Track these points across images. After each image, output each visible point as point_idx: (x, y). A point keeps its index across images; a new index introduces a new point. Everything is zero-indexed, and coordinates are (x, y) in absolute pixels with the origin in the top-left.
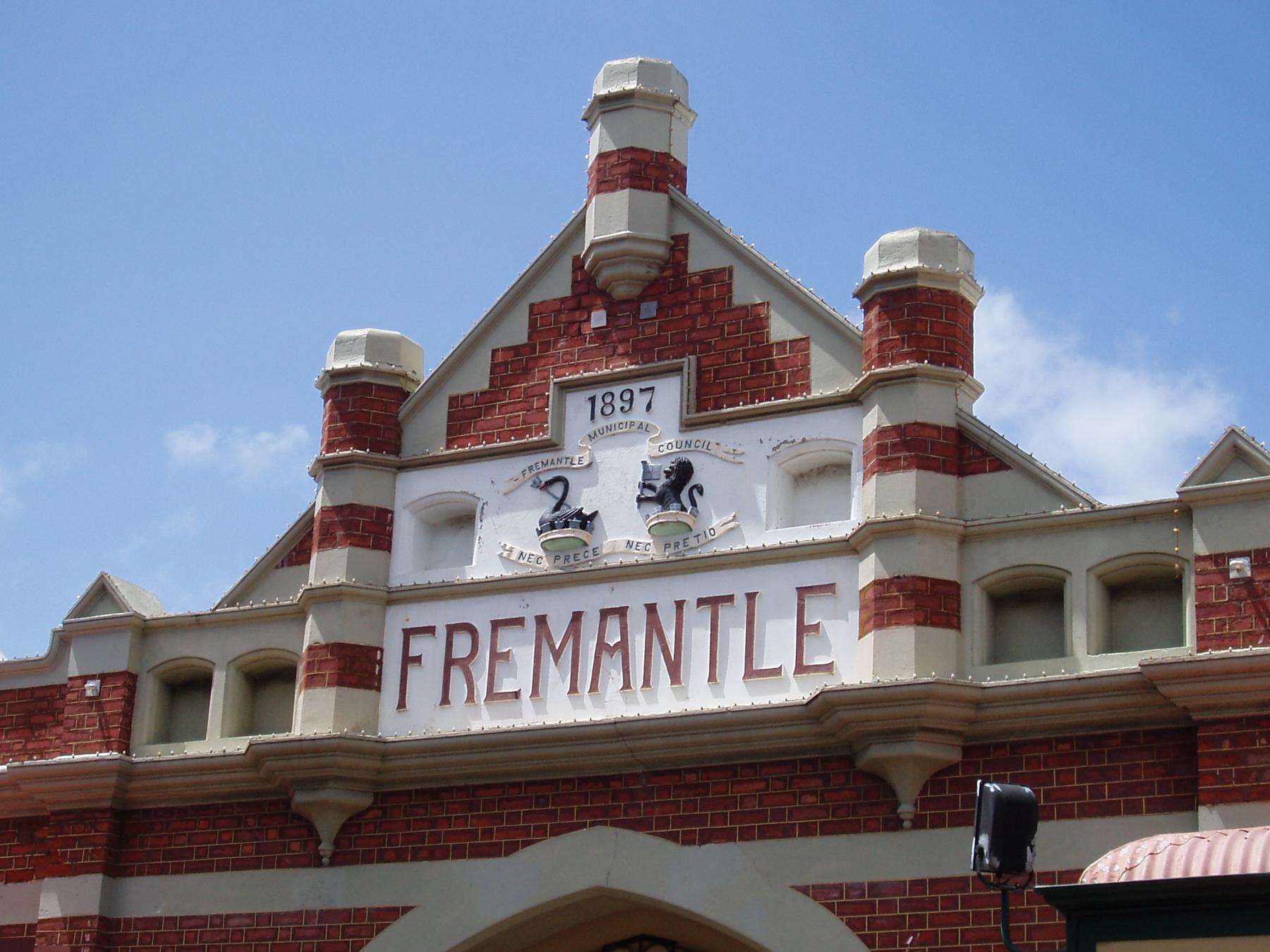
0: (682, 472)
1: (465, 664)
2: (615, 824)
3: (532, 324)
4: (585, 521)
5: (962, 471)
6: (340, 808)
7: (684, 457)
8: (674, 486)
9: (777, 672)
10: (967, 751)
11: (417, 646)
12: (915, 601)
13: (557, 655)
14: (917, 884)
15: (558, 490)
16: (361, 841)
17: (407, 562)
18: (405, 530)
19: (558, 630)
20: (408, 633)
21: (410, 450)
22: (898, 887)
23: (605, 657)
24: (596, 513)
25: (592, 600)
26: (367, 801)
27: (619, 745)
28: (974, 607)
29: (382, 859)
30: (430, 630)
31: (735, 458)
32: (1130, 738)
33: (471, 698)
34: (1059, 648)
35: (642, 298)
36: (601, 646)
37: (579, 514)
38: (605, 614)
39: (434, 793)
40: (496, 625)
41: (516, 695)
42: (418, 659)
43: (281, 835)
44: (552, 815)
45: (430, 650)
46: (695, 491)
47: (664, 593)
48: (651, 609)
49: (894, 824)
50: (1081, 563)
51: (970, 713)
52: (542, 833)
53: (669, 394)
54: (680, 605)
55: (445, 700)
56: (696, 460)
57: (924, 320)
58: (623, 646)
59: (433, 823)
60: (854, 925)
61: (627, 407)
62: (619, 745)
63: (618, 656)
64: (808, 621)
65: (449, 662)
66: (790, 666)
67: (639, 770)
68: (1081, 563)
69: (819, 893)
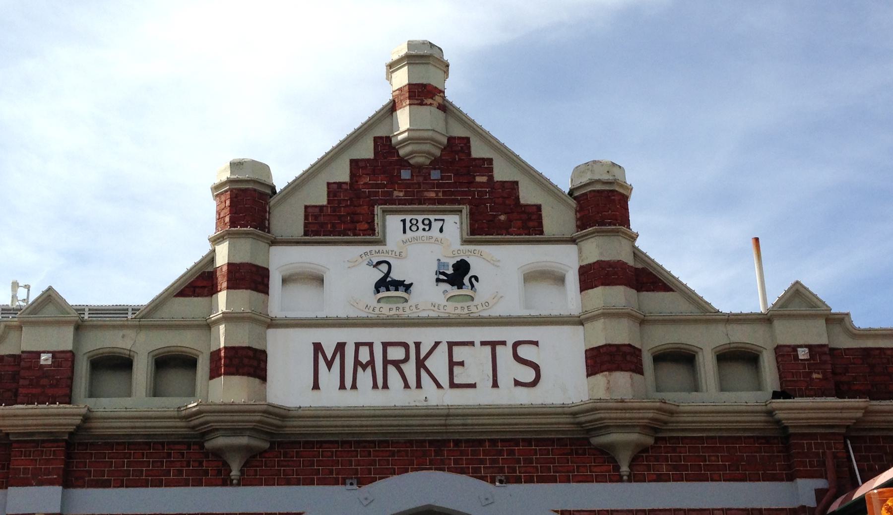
0: (462, 267)
15: (384, 268)
17: (280, 301)
24: (411, 284)
31: (495, 263)
46: (473, 280)
61: (427, 228)
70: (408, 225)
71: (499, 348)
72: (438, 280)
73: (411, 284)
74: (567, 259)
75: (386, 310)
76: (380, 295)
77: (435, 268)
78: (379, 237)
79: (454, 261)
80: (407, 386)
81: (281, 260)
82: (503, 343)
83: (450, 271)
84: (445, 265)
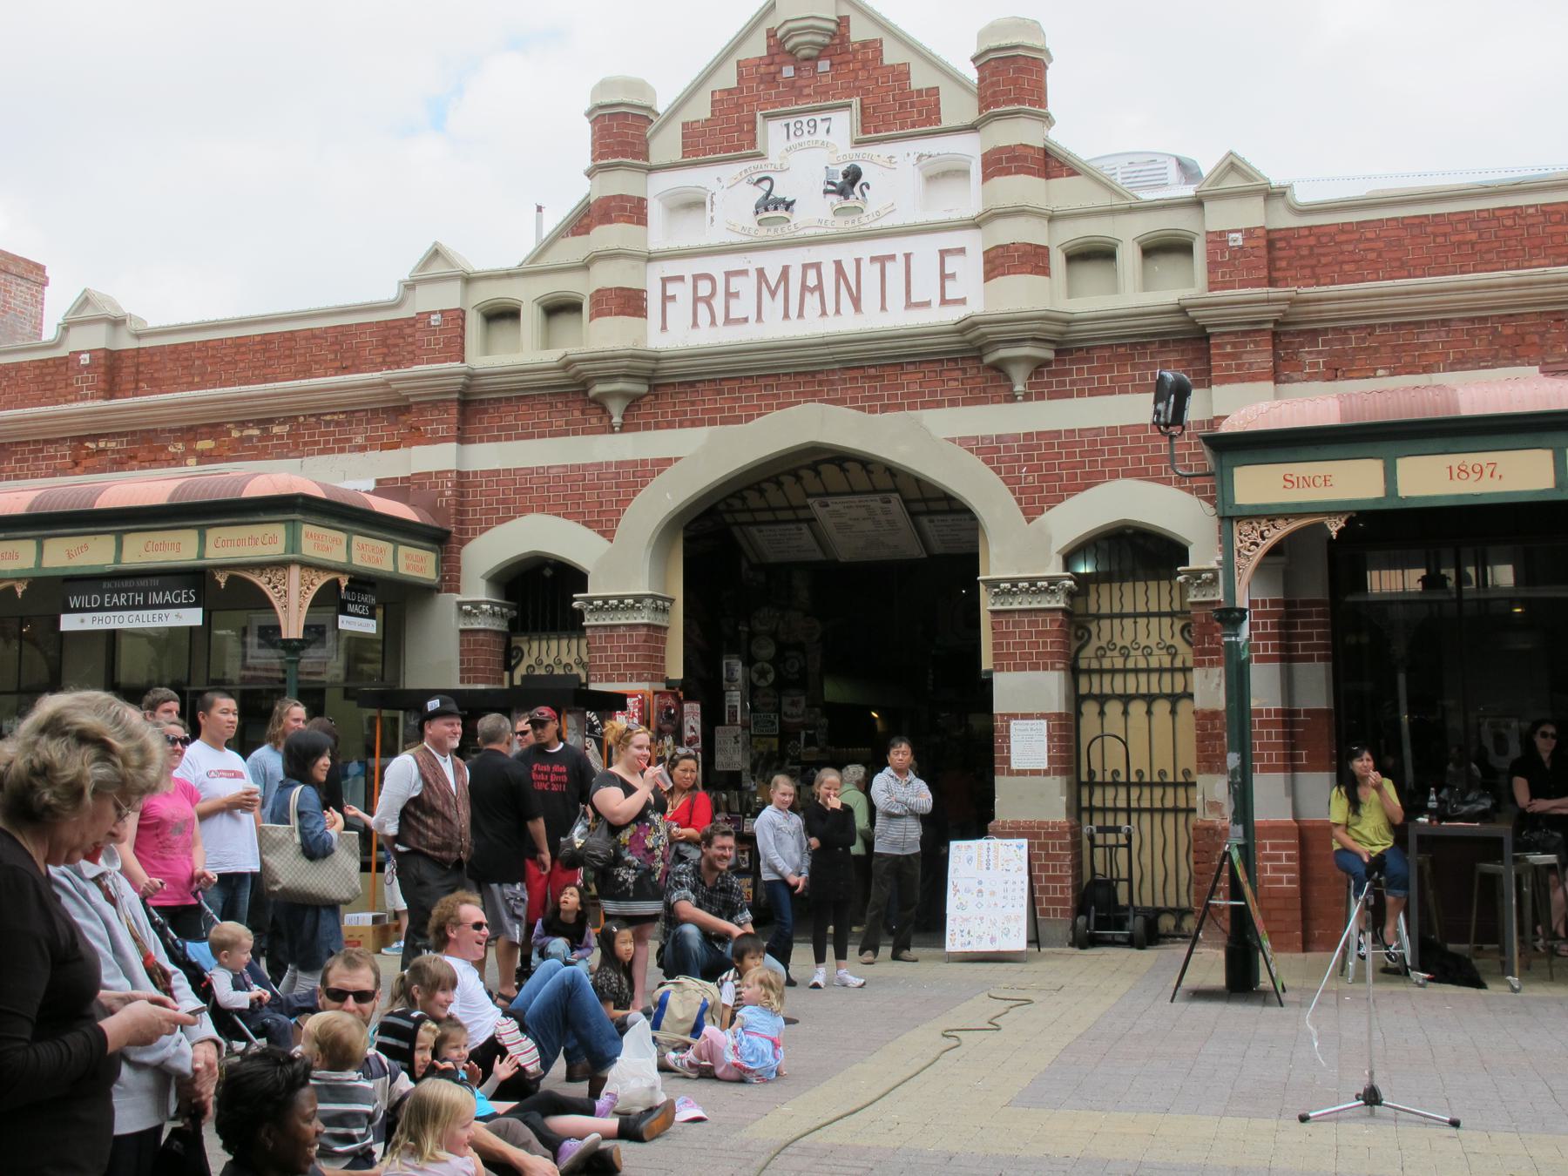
0: (853, 176)
1: (708, 301)
2: (821, 401)
3: (740, 75)
5: (1047, 175)
7: (859, 164)
9: (927, 304)
11: (672, 289)
13: (773, 294)
14: (1028, 435)
15: (766, 185)
17: (659, 232)
18: (655, 210)
19: (773, 277)
20: (665, 281)
21: (655, 160)
22: (1015, 437)
23: (808, 295)
24: (793, 203)
25: (796, 258)
28: (1057, 260)
29: (658, 426)
30: (681, 278)
33: (713, 323)
34: (1115, 289)
35: (818, 58)
36: (804, 287)
37: (783, 201)
38: (805, 267)
39: (692, 384)
40: (728, 274)
41: (746, 320)
42: (673, 298)
43: (583, 413)
44: (776, 396)
45: (682, 292)
47: (847, 253)
48: (838, 264)
49: (1012, 398)
50: (1128, 234)
52: (770, 408)
53: (843, 123)
54: (858, 261)
55: (695, 324)
56: (862, 166)
57: (1013, 76)
58: (819, 287)
59: (693, 403)
60: (987, 461)
63: (817, 294)
64: (947, 271)
65: (696, 300)
66: (936, 299)
67: (836, 366)
68: (1128, 234)
69: (964, 442)
70: (792, 129)
71: (889, 265)
72: (826, 192)
73: (793, 203)
74: (970, 149)
75: (764, 234)
76: (759, 217)
77: (824, 178)
78: (759, 148)
79: (844, 167)
80: (824, 313)
81: (657, 189)
82: (892, 257)
83: (839, 180)
84: (834, 173)
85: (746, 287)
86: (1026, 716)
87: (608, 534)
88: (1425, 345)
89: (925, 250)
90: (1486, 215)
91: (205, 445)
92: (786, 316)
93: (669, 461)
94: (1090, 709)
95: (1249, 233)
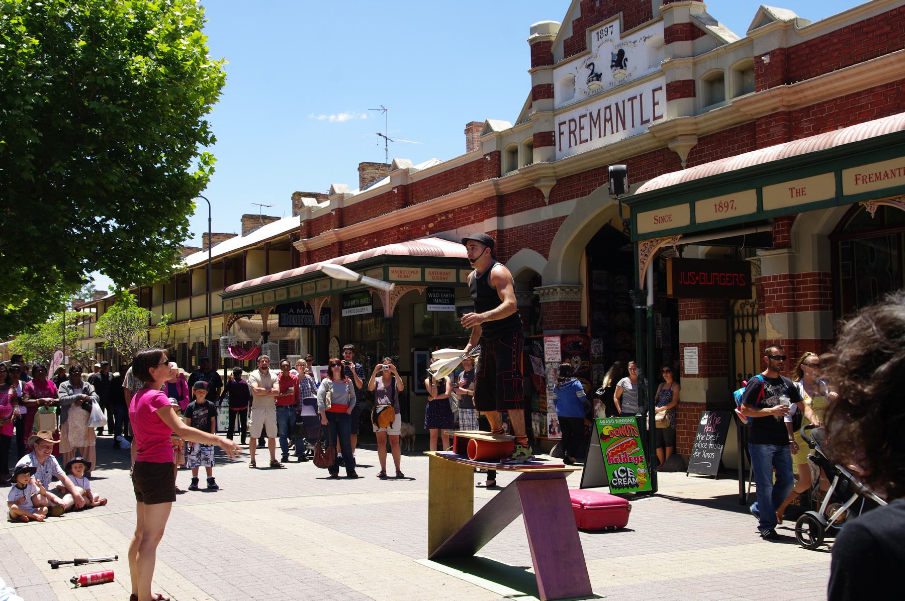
1: (573, 132)
4: (598, 77)
6: (548, 186)
8: (619, 60)
10: (699, 140)
12: (679, 90)
15: (591, 67)
16: (556, 197)
19: (595, 116)
25: (601, 104)
26: (555, 183)
27: (608, 154)
28: (700, 88)
32: (742, 127)
36: (606, 120)
48: (617, 104)
51: (694, 127)
52: (596, 186)
56: (625, 49)
58: (611, 119)
62: (608, 154)
64: (656, 101)
65: (570, 133)
85: (586, 122)
86: (690, 345)
87: (546, 256)
88: (862, 107)
89: (646, 89)
90: (895, 12)
91: (431, 225)
92: (600, 137)
93: (563, 218)
94: (739, 338)
95: (772, 54)
